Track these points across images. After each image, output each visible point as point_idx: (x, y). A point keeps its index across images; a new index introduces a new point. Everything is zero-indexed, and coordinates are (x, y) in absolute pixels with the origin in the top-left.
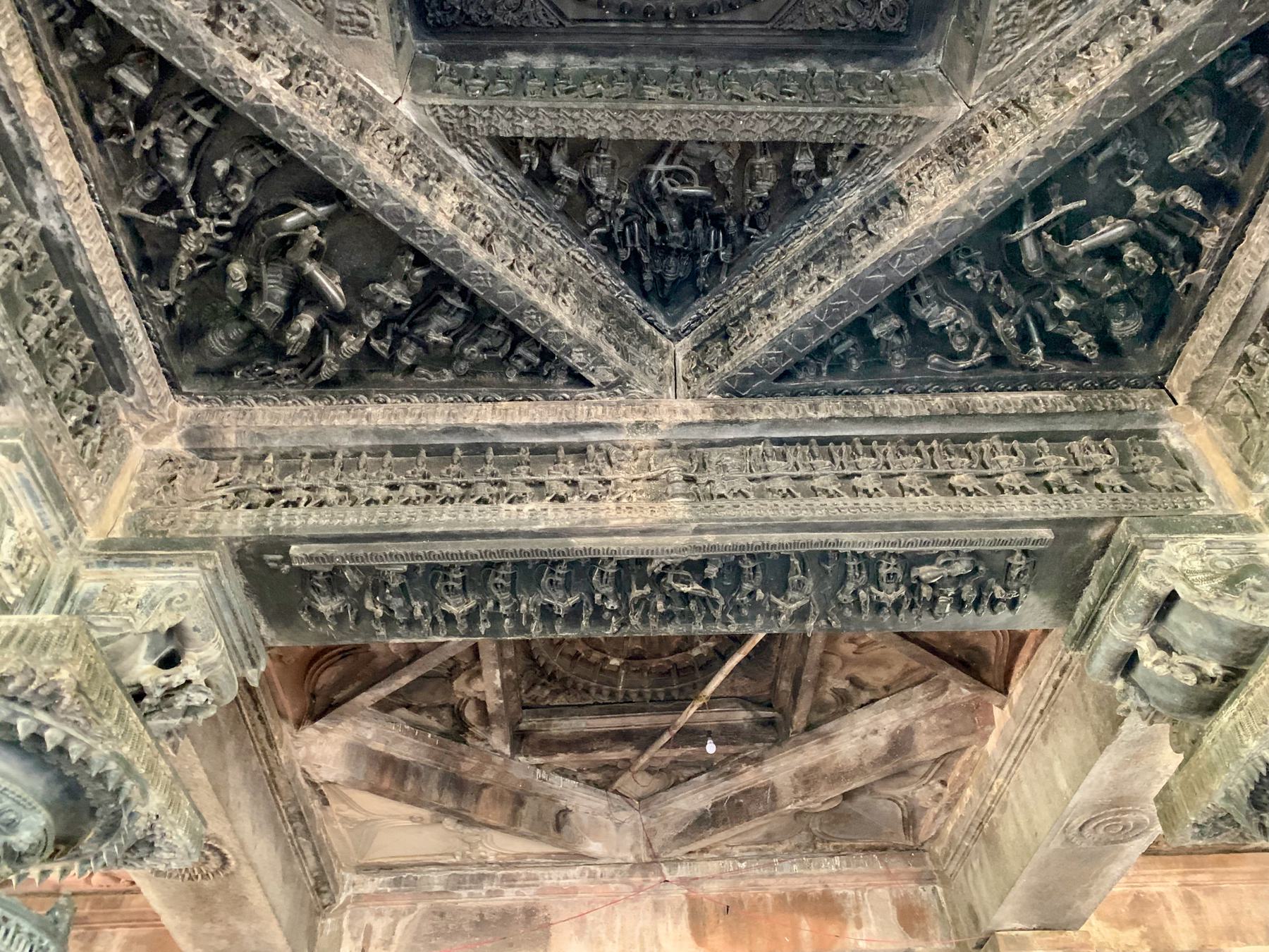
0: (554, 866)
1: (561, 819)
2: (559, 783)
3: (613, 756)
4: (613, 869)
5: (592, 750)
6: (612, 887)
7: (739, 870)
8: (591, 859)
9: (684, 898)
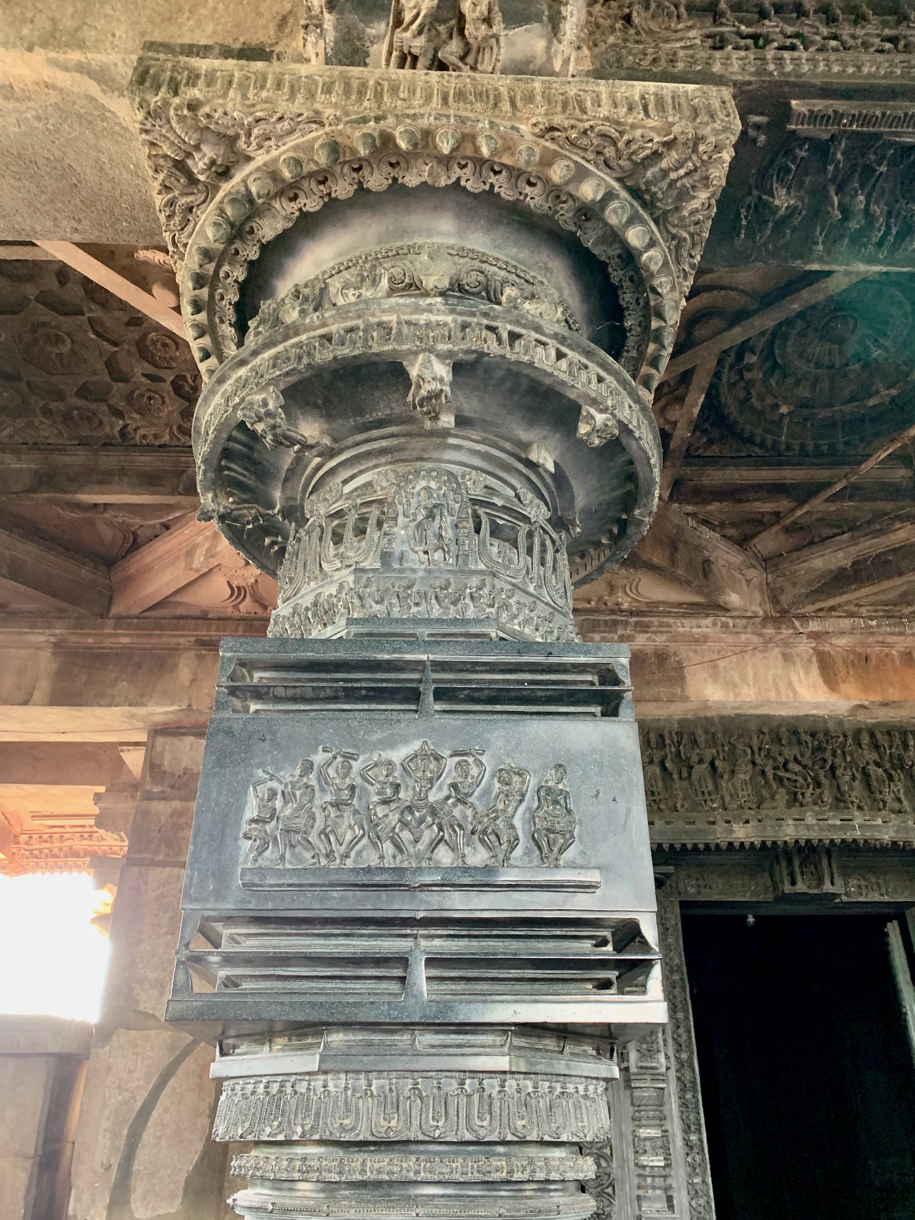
0: (683, 616)
1: (706, 568)
2: (707, 533)
3: (768, 507)
4: (744, 621)
5: (748, 501)
6: (743, 637)
7: (871, 627)
8: (724, 609)
9: (811, 651)
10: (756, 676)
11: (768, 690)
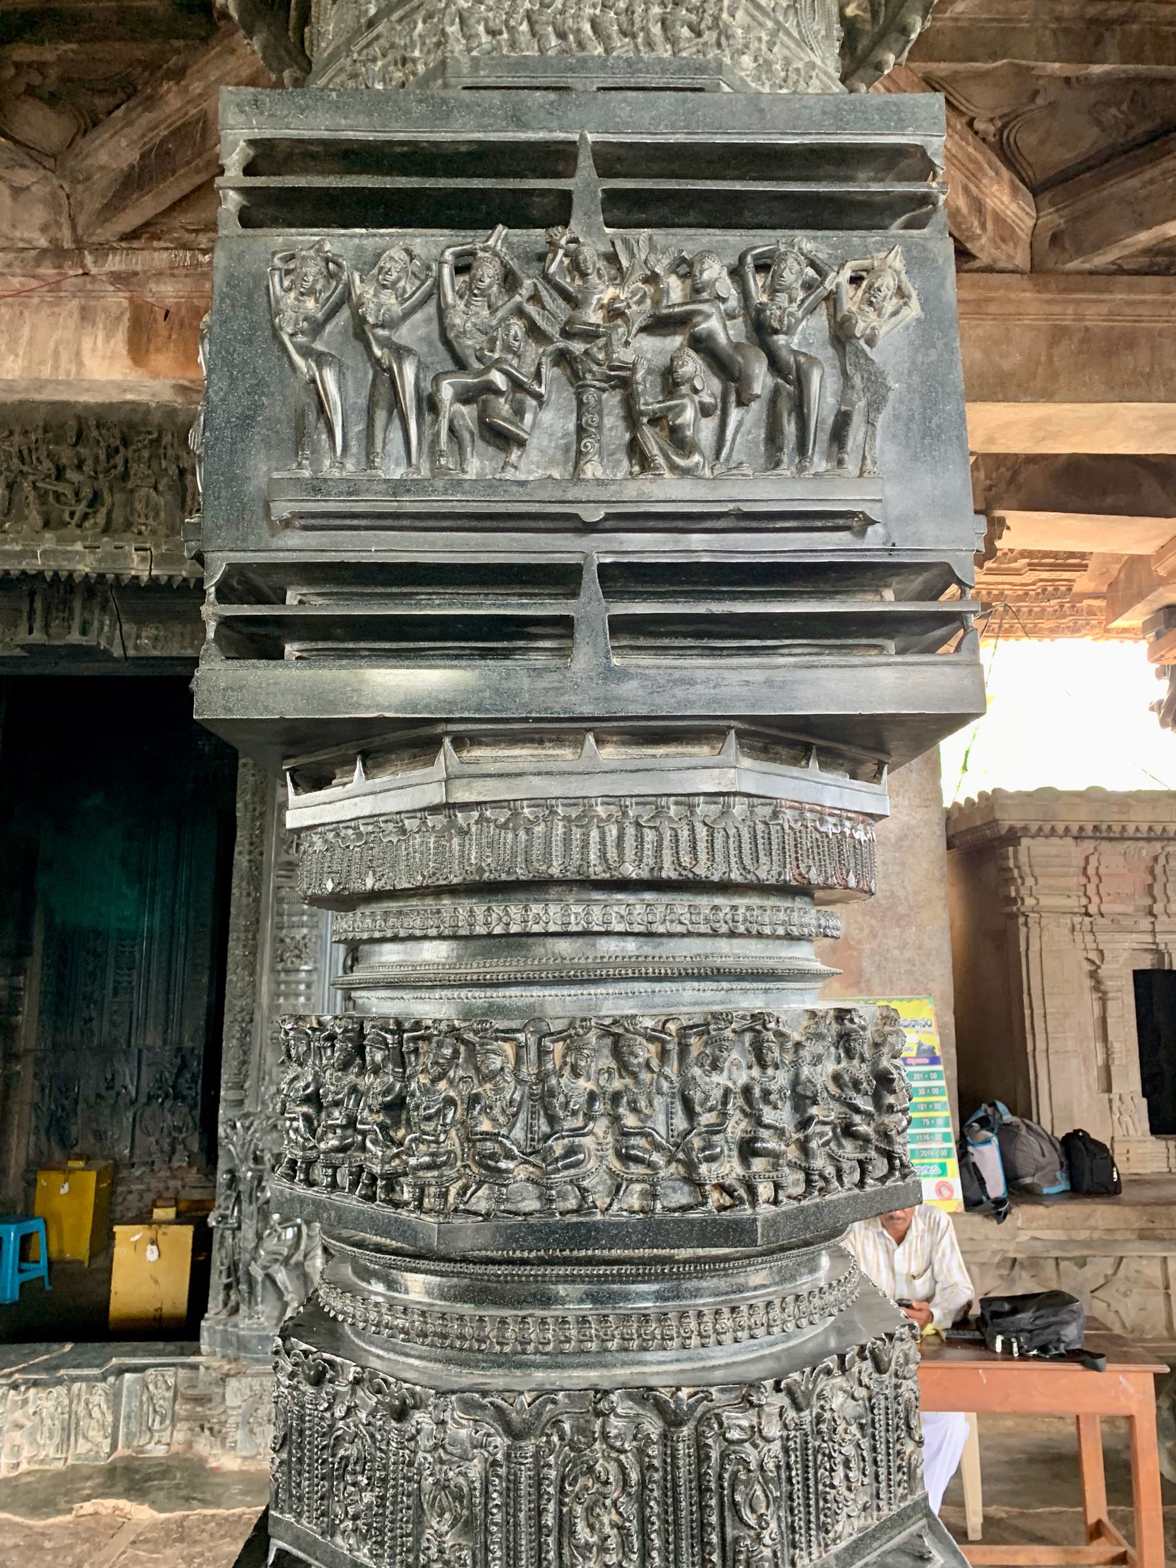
7: (201, 264)
9: (126, 303)
10: (31, 342)
11: (43, 362)
